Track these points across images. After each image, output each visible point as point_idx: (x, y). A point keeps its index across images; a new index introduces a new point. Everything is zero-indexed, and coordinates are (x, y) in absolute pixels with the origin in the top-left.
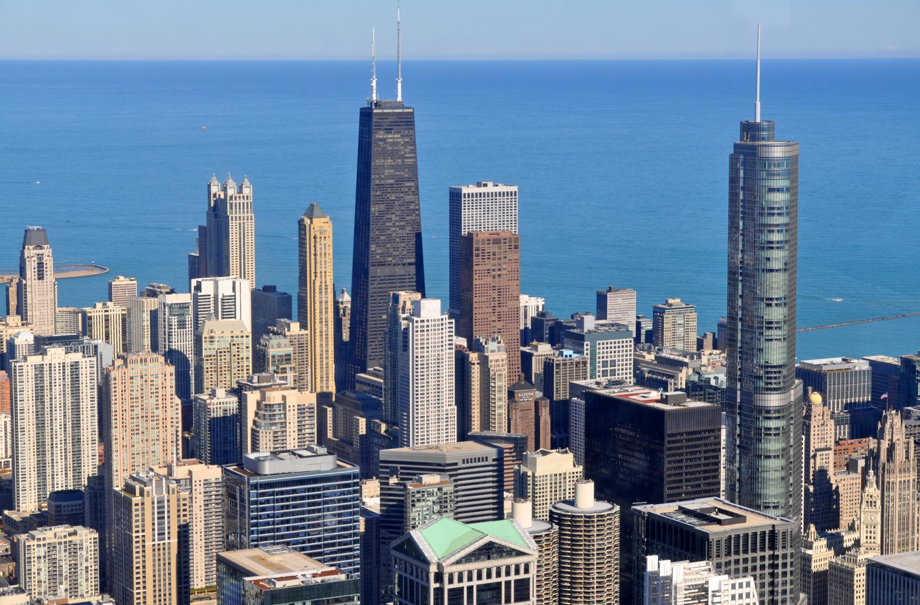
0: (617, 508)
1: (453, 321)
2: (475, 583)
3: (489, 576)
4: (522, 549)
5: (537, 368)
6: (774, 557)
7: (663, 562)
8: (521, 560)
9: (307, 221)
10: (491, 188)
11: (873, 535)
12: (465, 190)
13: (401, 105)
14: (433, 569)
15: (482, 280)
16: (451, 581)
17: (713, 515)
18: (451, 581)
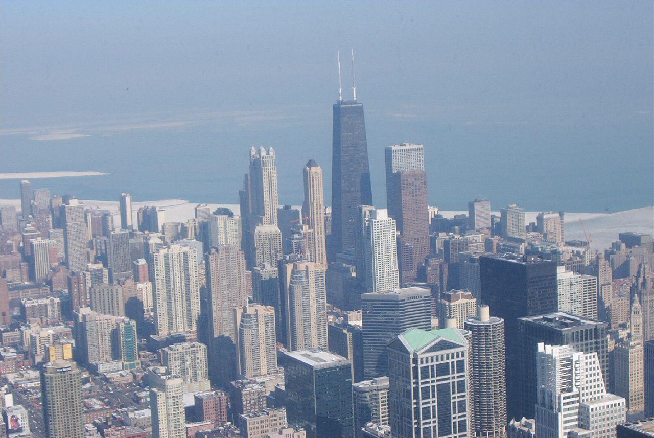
0: (502, 320)
1: (395, 221)
2: (435, 363)
3: (442, 359)
4: (460, 344)
5: (439, 246)
6: (596, 343)
7: (546, 346)
8: (459, 350)
9: (308, 169)
10: (408, 147)
11: (638, 330)
12: (394, 148)
13: (356, 103)
14: (412, 356)
15: (406, 198)
16: (422, 363)
17: (563, 321)
18: (422, 363)
